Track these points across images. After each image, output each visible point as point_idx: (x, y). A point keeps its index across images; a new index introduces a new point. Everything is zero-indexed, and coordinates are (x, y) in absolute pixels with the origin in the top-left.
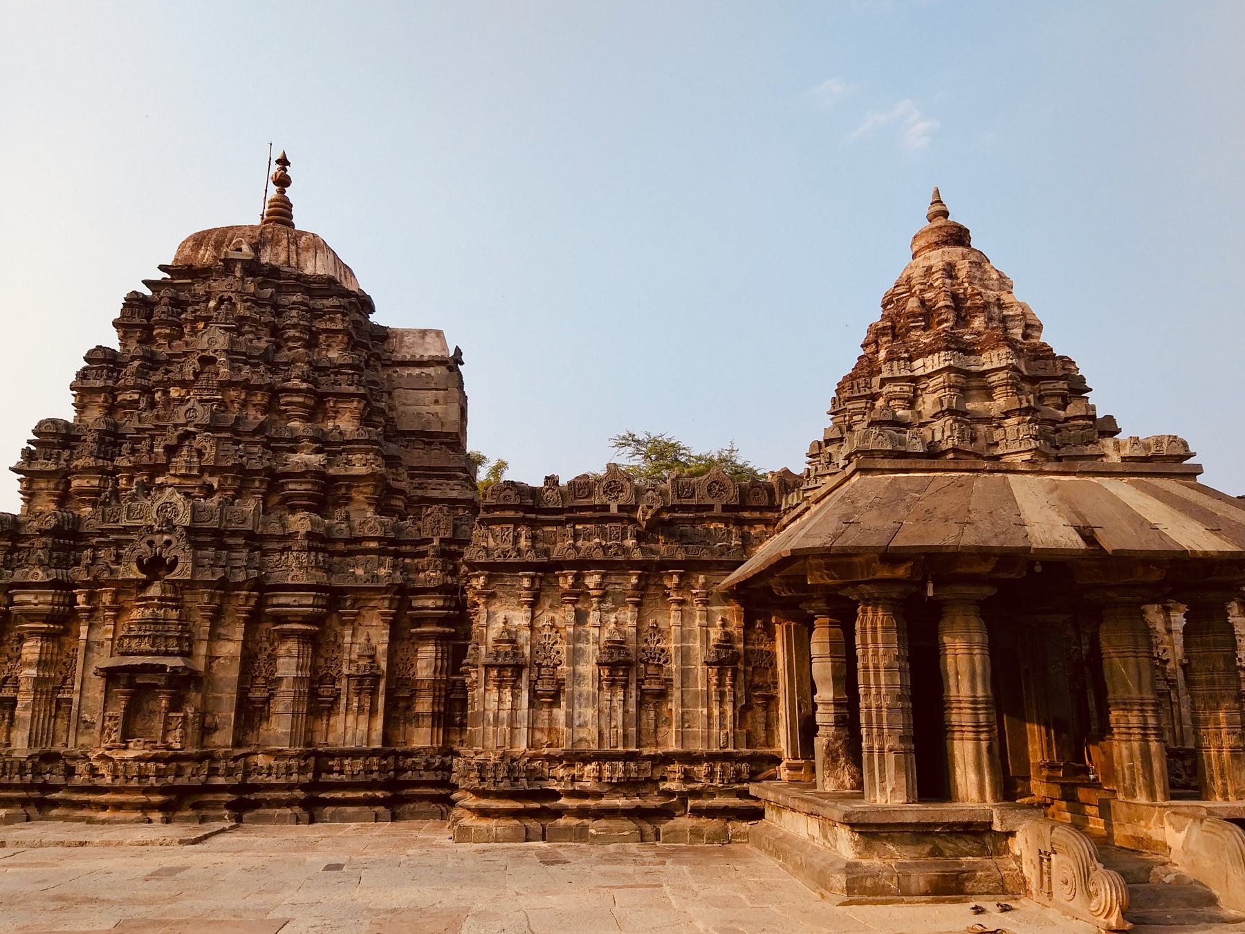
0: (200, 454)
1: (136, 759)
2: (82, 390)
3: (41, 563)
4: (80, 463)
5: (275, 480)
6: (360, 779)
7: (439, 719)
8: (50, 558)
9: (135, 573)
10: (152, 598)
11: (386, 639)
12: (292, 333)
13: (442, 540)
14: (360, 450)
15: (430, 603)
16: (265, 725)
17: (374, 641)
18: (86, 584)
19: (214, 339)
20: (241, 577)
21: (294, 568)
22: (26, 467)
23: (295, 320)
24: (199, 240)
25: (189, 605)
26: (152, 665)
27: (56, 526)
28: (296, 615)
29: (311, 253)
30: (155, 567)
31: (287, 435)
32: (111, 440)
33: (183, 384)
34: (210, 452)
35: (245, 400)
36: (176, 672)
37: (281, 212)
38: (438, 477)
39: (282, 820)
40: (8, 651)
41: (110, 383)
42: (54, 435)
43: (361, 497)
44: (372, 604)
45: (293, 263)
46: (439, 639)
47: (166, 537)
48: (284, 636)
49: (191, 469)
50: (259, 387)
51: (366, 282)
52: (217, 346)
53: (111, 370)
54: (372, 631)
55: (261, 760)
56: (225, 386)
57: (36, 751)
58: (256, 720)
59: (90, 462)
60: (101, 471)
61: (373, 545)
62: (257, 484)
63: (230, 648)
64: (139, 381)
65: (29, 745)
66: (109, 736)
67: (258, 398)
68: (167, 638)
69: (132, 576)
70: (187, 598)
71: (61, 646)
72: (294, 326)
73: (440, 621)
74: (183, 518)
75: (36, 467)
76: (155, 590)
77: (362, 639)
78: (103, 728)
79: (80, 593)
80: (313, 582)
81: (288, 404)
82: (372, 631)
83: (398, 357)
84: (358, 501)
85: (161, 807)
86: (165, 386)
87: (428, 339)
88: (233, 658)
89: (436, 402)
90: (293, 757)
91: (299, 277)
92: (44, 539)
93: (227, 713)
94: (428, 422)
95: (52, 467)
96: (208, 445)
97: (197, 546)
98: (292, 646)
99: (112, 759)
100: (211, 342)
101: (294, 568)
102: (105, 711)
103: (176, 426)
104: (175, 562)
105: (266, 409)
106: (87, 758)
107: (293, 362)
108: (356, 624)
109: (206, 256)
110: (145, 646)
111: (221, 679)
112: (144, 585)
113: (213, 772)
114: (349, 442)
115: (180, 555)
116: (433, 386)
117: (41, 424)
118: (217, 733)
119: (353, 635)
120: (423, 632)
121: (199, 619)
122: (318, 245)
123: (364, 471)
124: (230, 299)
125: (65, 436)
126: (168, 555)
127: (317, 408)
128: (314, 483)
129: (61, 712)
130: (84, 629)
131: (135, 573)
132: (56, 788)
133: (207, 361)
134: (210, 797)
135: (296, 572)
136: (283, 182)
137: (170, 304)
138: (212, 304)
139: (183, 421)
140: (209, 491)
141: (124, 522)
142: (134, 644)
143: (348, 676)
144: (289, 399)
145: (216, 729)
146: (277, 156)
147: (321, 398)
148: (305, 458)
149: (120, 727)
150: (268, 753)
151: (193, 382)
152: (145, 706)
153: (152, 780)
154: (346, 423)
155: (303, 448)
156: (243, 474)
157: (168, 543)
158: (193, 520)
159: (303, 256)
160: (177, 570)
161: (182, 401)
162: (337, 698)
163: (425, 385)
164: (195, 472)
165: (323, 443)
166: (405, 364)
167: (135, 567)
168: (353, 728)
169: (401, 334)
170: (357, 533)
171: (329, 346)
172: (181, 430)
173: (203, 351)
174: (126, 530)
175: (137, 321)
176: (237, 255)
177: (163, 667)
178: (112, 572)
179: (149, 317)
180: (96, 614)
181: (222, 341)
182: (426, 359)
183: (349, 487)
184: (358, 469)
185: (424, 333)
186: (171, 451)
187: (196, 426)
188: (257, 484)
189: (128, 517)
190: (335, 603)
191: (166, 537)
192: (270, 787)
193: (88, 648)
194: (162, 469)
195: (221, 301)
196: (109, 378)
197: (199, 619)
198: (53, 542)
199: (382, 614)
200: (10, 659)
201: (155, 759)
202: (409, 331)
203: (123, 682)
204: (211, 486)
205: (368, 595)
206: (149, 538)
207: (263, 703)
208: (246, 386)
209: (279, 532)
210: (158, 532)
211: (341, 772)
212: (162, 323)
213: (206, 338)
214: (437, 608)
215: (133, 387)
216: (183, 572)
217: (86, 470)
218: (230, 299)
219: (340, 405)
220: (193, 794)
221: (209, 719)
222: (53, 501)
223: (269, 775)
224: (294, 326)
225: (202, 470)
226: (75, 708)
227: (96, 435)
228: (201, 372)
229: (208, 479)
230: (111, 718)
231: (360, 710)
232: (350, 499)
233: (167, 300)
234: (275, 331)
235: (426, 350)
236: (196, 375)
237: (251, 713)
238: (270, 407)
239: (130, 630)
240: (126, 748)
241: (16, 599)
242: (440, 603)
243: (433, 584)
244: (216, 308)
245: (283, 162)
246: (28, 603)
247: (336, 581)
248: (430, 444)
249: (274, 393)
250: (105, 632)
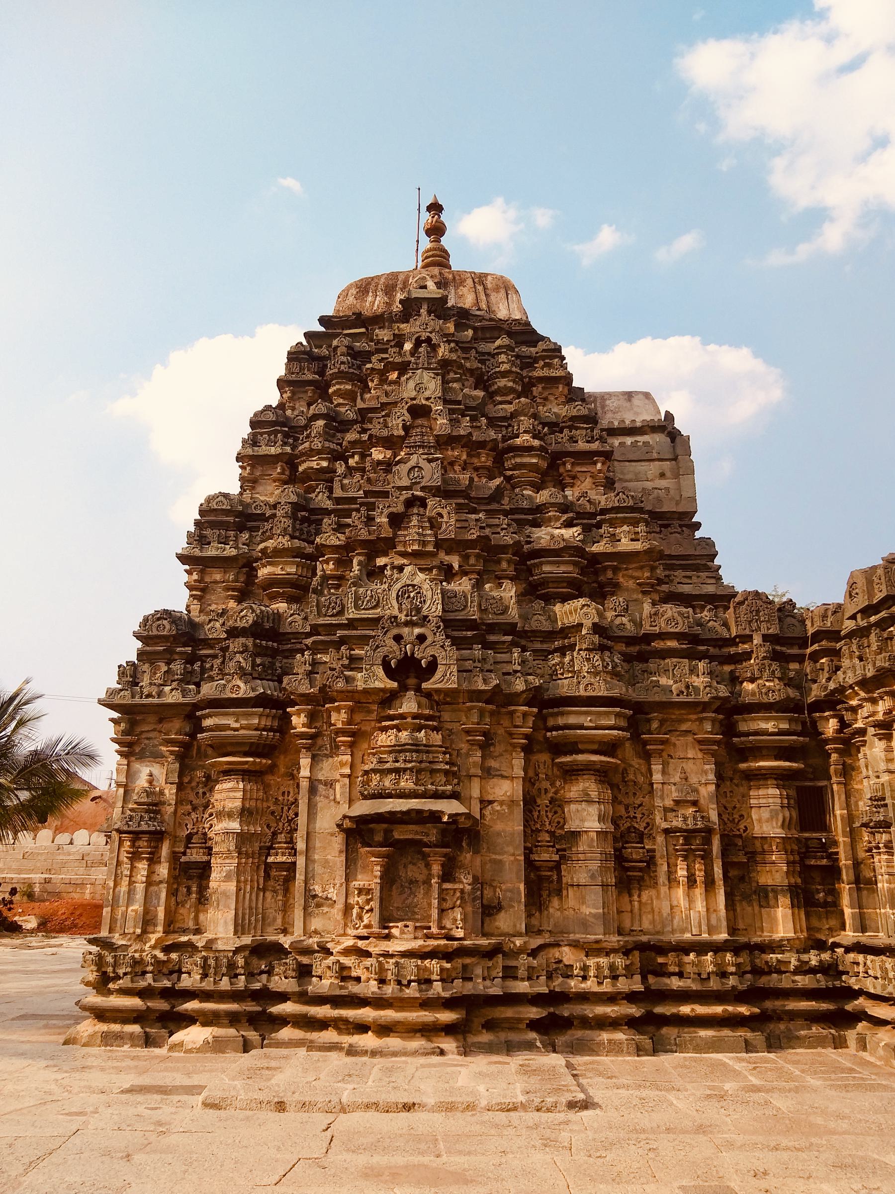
0: (434, 524)
1: (408, 954)
2: (252, 461)
3: (243, 673)
4: (270, 544)
5: (526, 559)
6: (714, 984)
7: (798, 895)
8: (254, 665)
9: (382, 682)
10: (402, 717)
11: (711, 777)
12: (502, 382)
13: (765, 638)
14: (624, 521)
15: (770, 726)
16: (555, 902)
17: (693, 779)
18: (307, 699)
20: (519, 685)
21: (582, 674)
22: (197, 552)
23: (505, 367)
25: (448, 726)
26: (419, 812)
27: (255, 623)
28: (590, 740)
29: (502, 292)
30: (408, 671)
31: (525, 504)
33: (390, 442)
35: (465, 462)
36: (455, 822)
38: (684, 568)
39: (615, 1048)
40: (192, 797)
41: (288, 449)
42: (226, 512)
43: (631, 584)
44: (684, 727)
45: (484, 306)
46: (782, 778)
47: (417, 631)
48: (571, 773)
49: (424, 543)
50: (482, 445)
52: (427, 394)
53: (286, 435)
54: (689, 766)
55: (568, 955)
56: (445, 442)
57: (247, 940)
58: (545, 894)
59: (285, 542)
60: (297, 553)
61: (672, 644)
62: (504, 565)
63: (507, 789)
64: (327, 444)
65: (236, 933)
66: (360, 918)
68: (433, 772)
69: (378, 685)
70: (446, 716)
71: (266, 787)
72: (504, 374)
73: (783, 753)
74: (434, 608)
75: (212, 551)
76: (409, 705)
77: (676, 778)
78: (348, 909)
79: (298, 713)
80: (615, 693)
81: (516, 467)
82: (689, 766)
84: (627, 590)
85: (449, 1030)
87: (636, 401)
88: (512, 803)
89: (662, 475)
90: (614, 951)
92: (242, 640)
93: (513, 884)
94: (659, 500)
95: (230, 551)
96: (444, 512)
97: (458, 643)
98: (588, 785)
99: (368, 954)
100: (419, 388)
101: (582, 674)
102: (347, 880)
103: (401, 489)
104: (433, 665)
106: (328, 952)
107: (514, 415)
108: (665, 754)
109: (375, 303)
110: (407, 783)
111: (499, 834)
112: (389, 698)
113: (510, 973)
114: (603, 512)
115: (441, 655)
116: (655, 456)
117: (209, 500)
118: (502, 914)
119: (664, 772)
120: (760, 768)
121: (464, 747)
124: (428, 340)
125: (240, 514)
126: (423, 655)
128: (575, 564)
129: (271, 883)
130: (305, 762)
131: (382, 682)
132: (283, 997)
133: (419, 412)
134: (509, 1012)
135: (589, 679)
136: (436, 231)
137: (349, 354)
138: (408, 346)
139: (406, 482)
140: (448, 573)
141: (352, 613)
142: (388, 782)
143: (667, 831)
144: (518, 460)
145: (499, 908)
146: (427, 201)
147: (556, 459)
149: (375, 904)
150: (575, 945)
151: (403, 438)
152: (402, 873)
153: (438, 987)
155: (550, 519)
156: (489, 551)
157: (421, 638)
158: (444, 610)
159: (493, 297)
160: (438, 675)
162: (650, 861)
164: (430, 548)
165: (574, 515)
167: (380, 671)
168: (688, 908)
169: (603, 397)
170: (647, 628)
171: (546, 399)
172: (406, 495)
173: (412, 399)
174: (352, 624)
175: (310, 376)
176: (422, 294)
177: (435, 817)
178: (348, 680)
179: (321, 373)
180: (320, 742)
182: (638, 424)
183: (615, 570)
184: (626, 545)
185: (629, 395)
186: (397, 521)
187: (423, 489)
188: (504, 565)
189: (357, 607)
190: (643, 723)
191: (417, 631)
192: (585, 997)
193: (313, 790)
194: (386, 545)
195: (418, 343)
196: (285, 444)
197: (464, 747)
198: (255, 645)
199: (700, 742)
200: (194, 809)
201: (432, 954)
202: (610, 394)
203: (379, 837)
204: (450, 567)
205: (677, 713)
206: (395, 631)
207: (551, 869)
209: (546, 626)
210: (407, 624)
211: (680, 975)
212: (341, 376)
213: (411, 384)
214: (781, 733)
215: (319, 452)
216: (445, 678)
217: (278, 553)
218: (428, 340)
219: (578, 469)
220: (491, 1007)
221: (488, 893)
222: (232, 597)
223: (585, 978)
224: (504, 374)
225: (438, 544)
226: (300, 876)
227: (288, 508)
228: (412, 427)
229: (443, 556)
230: (360, 891)
231: (691, 881)
232: (617, 586)
233: (344, 350)
235: (637, 414)
236: (406, 428)
237: (543, 884)
239: (381, 761)
240: (388, 937)
241: (207, 722)
242: (785, 726)
243: (772, 698)
244: (414, 352)
245: (435, 208)
246: (227, 727)
247: (634, 695)
248: (666, 526)
250: (337, 767)
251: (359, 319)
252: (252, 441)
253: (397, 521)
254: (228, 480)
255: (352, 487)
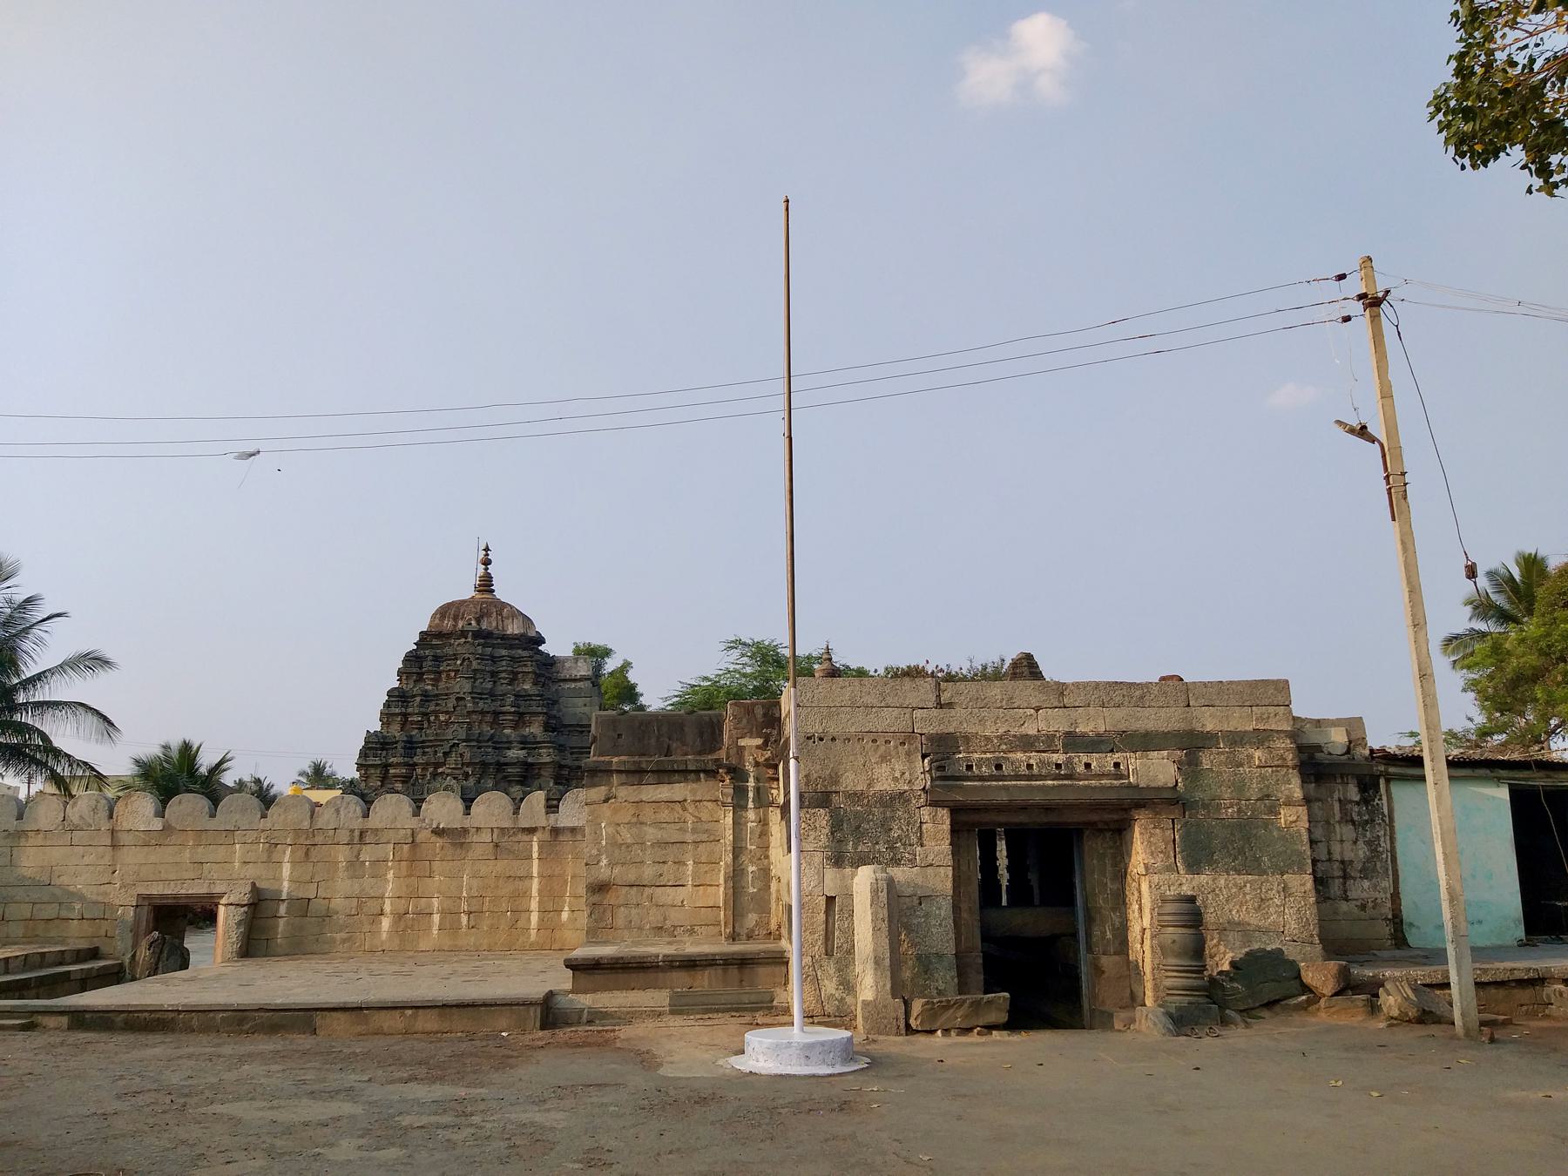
19: (462, 686)
24: (443, 612)
32: (411, 746)
33: (447, 713)
34: (467, 756)
37: (486, 584)
51: (541, 627)
59: (401, 760)
60: (406, 764)
67: (489, 718)
83: (562, 676)
86: (436, 713)
91: (504, 637)
105: (492, 725)
109: (448, 624)
122: (516, 614)
123: (548, 760)
127: (520, 719)
136: (487, 562)
140: (466, 776)
147: (521, 715)
148: (515, 753)
154: (535, 729)
156: (484, 765)
161: (447, 723)
163: (577, 694)
165: (525, 743)
166: (565, 680)
181: (467, 687)
186: (446, 754)
208: (482, 713)
212: (429, 672)
217: (398, 765)
234: (494, 674)
238: (495, 723)
245: (487, 549)
249: (496, 714)
251: (440, 635)
252: (387, 705)
253: (446, 754)
254: (376, 726)
255: (430, 733)
